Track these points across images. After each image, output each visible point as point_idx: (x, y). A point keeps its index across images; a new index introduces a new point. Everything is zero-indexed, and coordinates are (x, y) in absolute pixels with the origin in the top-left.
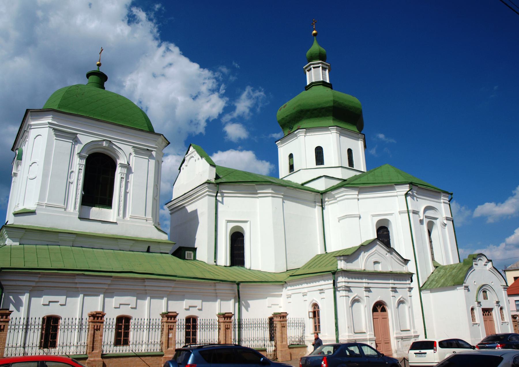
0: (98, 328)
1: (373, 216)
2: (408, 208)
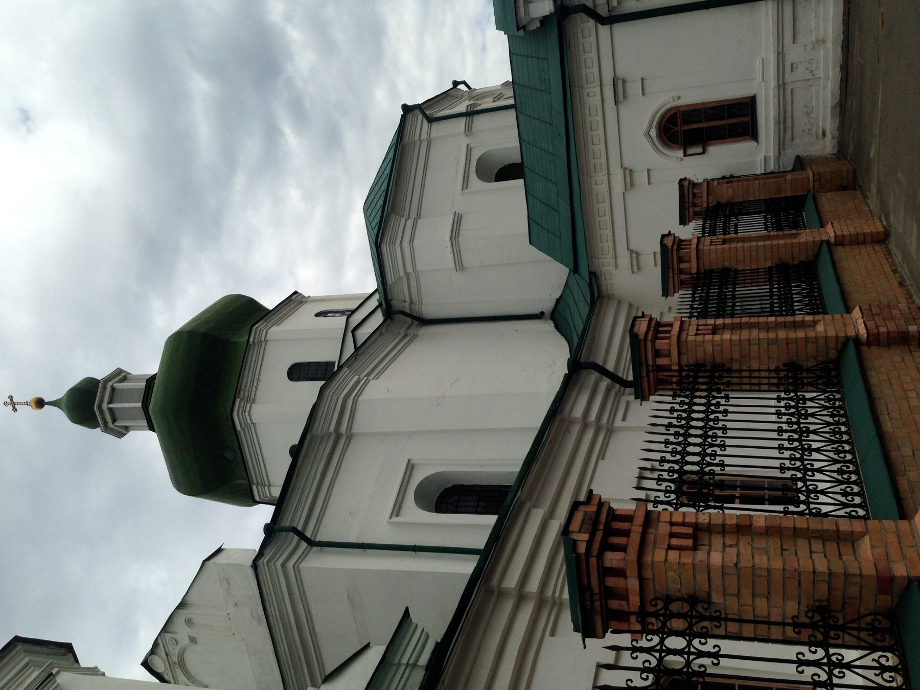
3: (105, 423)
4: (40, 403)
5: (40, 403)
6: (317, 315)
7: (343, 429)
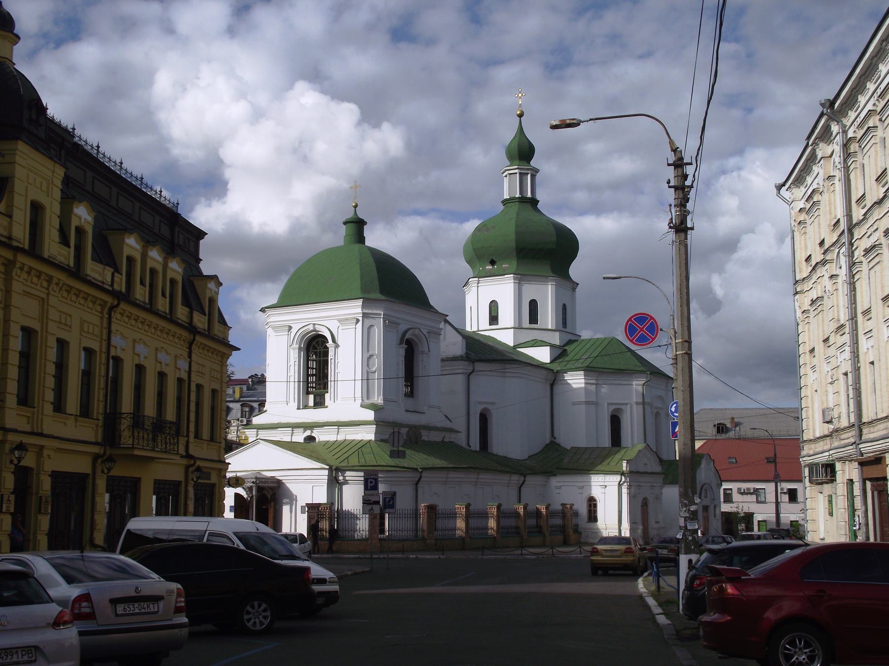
1: (609, 404)
2: (643, 399)
7: (508, 374)
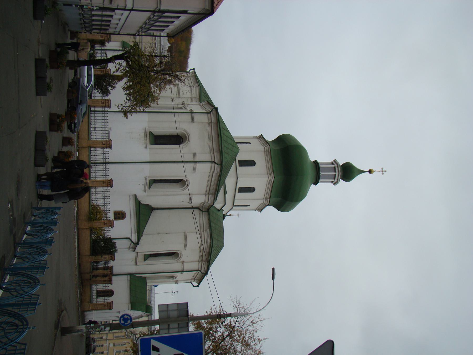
0: (104, 183)
3: (338, 167)
4: (370, 172)
5: (370, 172)
6: (249, 205)
